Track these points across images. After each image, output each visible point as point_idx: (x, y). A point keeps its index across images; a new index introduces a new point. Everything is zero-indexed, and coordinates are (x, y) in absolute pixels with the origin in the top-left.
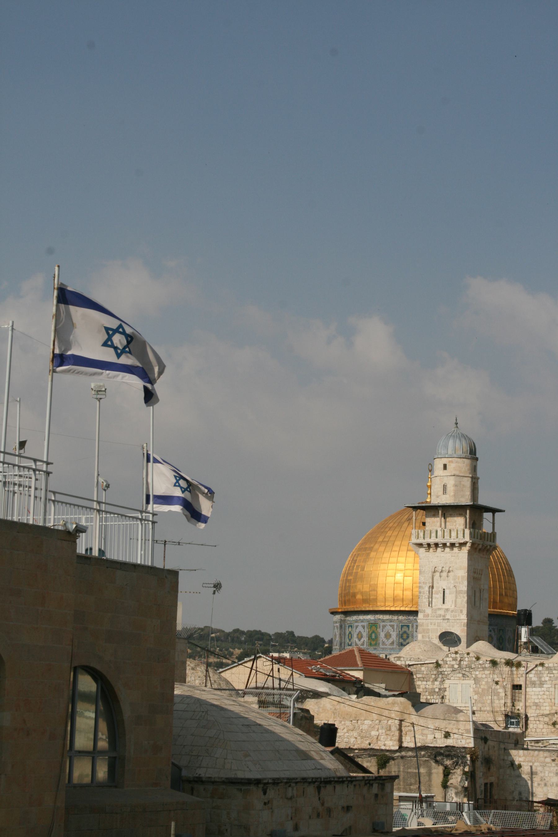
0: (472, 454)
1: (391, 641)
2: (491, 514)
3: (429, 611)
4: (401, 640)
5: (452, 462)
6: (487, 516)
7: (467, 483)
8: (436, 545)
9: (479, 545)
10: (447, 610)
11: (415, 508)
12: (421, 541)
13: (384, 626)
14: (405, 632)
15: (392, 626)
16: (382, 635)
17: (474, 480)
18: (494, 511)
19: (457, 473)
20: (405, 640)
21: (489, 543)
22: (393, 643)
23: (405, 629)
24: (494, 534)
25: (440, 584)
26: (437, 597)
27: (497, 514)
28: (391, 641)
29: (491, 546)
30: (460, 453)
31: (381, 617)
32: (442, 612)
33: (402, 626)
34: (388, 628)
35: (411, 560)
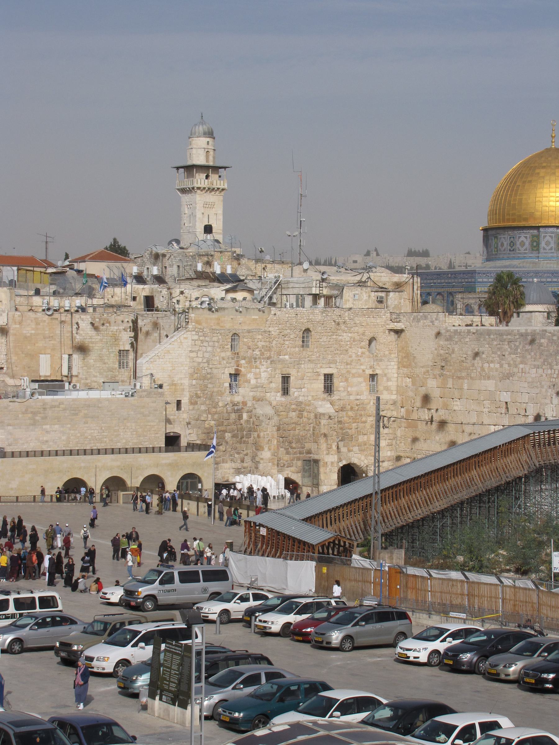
0: (210, 134)
1: (504, 248)
4: (509, 248)
5: (193, 140)
8: (184, 188)
9: (204, 188)
11: (178, 168)
14: (512, 242)
15: (504, 238)
16: (500, 244)
17: (207, 150)
18: (225, 168)
20: (512, 247)
22: (526, 249)
23: (512, 239)
28: (504, 248)
29: (218, 189)
31: (498, 231)
32: (188, 228)
33: (510, 238)
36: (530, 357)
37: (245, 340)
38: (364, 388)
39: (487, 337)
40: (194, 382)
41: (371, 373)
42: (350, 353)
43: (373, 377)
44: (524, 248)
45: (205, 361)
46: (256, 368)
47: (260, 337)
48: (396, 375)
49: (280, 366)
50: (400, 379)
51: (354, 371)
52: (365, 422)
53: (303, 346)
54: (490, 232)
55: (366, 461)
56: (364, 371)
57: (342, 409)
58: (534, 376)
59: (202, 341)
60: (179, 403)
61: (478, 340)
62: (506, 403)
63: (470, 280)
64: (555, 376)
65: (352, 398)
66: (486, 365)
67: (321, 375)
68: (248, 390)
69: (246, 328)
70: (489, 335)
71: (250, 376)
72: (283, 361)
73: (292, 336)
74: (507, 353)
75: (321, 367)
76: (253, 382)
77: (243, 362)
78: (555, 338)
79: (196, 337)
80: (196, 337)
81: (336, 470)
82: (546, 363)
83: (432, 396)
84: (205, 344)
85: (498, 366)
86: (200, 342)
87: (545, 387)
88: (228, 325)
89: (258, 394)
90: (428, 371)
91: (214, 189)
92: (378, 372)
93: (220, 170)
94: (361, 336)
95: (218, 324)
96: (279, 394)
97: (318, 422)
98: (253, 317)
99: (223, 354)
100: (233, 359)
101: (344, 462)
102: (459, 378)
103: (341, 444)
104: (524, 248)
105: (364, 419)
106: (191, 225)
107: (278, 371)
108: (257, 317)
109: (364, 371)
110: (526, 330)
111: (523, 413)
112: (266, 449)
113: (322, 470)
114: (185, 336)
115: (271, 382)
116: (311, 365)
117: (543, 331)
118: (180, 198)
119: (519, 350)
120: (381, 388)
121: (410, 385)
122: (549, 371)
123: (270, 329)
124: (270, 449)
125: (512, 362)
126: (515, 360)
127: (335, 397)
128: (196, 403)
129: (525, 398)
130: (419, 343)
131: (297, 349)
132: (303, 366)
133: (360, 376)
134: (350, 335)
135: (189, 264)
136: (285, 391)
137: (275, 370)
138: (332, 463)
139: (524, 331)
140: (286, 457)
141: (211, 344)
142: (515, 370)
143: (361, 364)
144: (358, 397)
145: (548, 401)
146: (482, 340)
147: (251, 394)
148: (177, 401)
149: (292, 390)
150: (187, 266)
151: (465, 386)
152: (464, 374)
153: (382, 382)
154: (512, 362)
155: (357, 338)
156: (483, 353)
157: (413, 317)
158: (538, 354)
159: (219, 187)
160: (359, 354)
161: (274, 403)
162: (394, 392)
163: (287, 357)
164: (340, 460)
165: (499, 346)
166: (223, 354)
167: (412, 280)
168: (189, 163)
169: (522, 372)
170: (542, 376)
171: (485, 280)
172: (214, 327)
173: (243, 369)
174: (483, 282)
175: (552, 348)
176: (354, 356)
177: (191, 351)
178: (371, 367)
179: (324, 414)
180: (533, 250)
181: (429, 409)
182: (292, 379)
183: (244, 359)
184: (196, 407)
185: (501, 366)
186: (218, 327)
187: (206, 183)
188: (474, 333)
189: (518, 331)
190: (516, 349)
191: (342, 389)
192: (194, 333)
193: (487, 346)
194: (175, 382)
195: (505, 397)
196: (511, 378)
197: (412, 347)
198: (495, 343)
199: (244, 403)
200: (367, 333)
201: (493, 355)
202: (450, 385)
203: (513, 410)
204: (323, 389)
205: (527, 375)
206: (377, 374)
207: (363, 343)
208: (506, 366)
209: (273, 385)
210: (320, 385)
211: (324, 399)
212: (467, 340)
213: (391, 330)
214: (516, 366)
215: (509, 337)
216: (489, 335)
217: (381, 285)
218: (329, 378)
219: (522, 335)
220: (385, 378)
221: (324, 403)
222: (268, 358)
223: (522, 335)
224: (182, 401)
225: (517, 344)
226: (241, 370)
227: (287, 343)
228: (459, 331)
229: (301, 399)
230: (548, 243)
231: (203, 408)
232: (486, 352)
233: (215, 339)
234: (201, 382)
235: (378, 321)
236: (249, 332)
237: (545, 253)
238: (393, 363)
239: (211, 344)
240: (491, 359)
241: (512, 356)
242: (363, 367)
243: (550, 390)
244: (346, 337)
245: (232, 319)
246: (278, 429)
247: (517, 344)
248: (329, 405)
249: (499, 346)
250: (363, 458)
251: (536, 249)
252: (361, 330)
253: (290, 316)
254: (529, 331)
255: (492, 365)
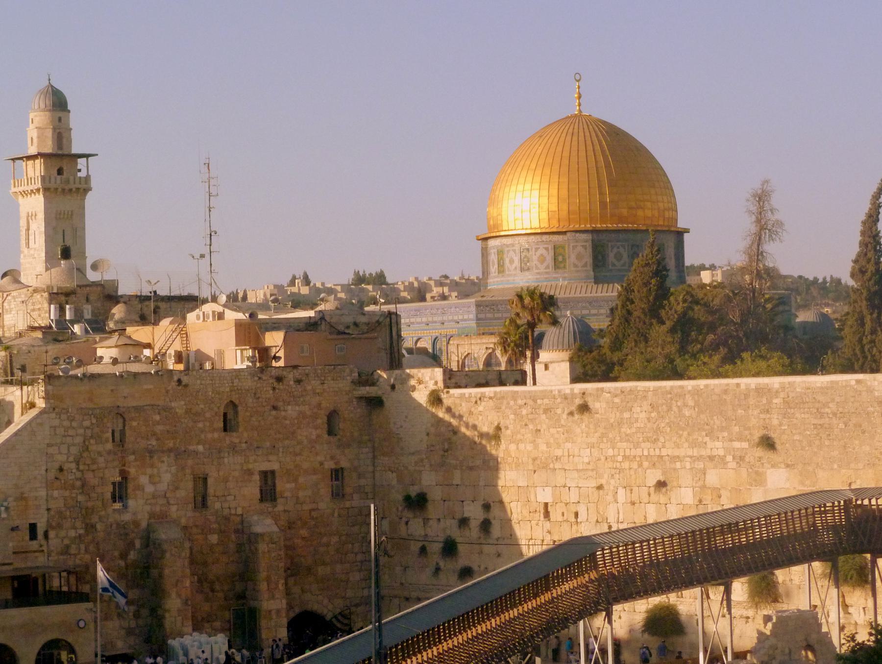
2: (85, 159)
3: (26, 250)
6: (81, 162)
7: (49, 133)
9: (57, 189)
10: (35, 249)
11: (13, 160)
12: (16, 190)
13: (508, 251)
16: (507, 261)
18: (87, 156)
19: (41, 125)
21: (78, 185)
22: (547, 267)
24: (87, 179)
25: (33, 226)
26: (31, 238)
27: (90, 158)
28: (514, 266)
29: (78, 189)
30: (42, 106)
32: (32, 252)
34: (512, 253)
35: (530, 178)
36: (578, 431)
37: (134, 424)
38: (323, 491)
39: (512, 403)
40: (56, 493)
41: (333, 467)
42: (299, 437)
43: (337, 474)
44: (545, 264)
45: (71, 459)
46: (152, 466)
47: (157, 418)
48: (370, 469)
49: (190, 462)
50: (377, 475)
51: (306, 465)
52: (328, 545)
53: (225, 430)
54: (491, 243)
55: (330, 607)
56: (321, 464)
57: (291, 525)
58: (586, 460)
59: (66, 429)
60: (33, 528)
61: (498, 408)
62: (546, 505)
63: (466, 317)
64: (620, 458)
65: (306, 507)
66: (513, 447)
67: (256, 473)
68: (141, 502)
69: (135, 404)
70: (515, 399)
71: (144, 480)
72: (196, 453)
73: (208, 415)
74: (544, 426)
75: (255, 461)
76: (150, 489)
77: (132, 457)
78: (617, 400)
79: (56, 422)
80: (56, 422)
81: (285, 621)
82: (605, 440)
83: (428, 497)
84: (71, 432)
85: (530, 447)
86: (62, 430)
87: (606, 476)
88: (107, 402)
89: (158, 509)
90: (422, 460)
91: (71, 190)
92: (344, 464)
93: (79, 160)
94: (315, 410)
95: (91, 400)
96: (191, 506)
97: (253, 548)
98: (145, 387)
99: (100, 448)
100: (115, 454)
101: (297, 610)
102: (471, 468)
103: (291, 581)
104: (545, 264)
105: (325, 540)
106: (37, 245)
107: (188, 471)
108: (151, 387)
109: (321, 464)
110: (572, 390)
111: (573, 520)
112: (174, 595)
113: (263, 623)
114: (39, 421)
115: (177, 488)
116: (239, 459)
117: (598, 389)
118: (18, 205)
119: (563, 422)
120: (348, 490)
121: (394, 482)
122: (610, 452)
123: (173, 404)
124: (179, 595)
125: (552, 441)
126: (557, 436)
127: (280, 508)
128: (59, 526)
129: (573, 497)
130: (406, 417)
131: (216, 435)
132: (226, 460)
133: (315, 472)
134: (297, 408)
135: (37, 307)
136: (202, 502)
137: (183, 469)
138: (278, 611)
139: (568, 391)
140: (206, 607)
141: (81, 431)
142: (559, 452)
143: (317, 454)
144: (313, 506)
145: (610, 498)
146: (503, 408)
147: (148, 508)
148: (31, 525)
149: (210, 500)
150: (33, 310)
151: (482, 483)
152: (478, 462)
153: (351, 482)
154: (552, 441)
155: (308, 413)
156: (507, 428)
157: (394, 376)
158: (591, 426)
159: (80, 186)
160: (314, 437)
161: (183, 521)
162: (370, 496)
163: (200, 448)
164: (290, 607)
165: (530, 417)
166: (100, 448)
167: (388, 319)
168: (33, 151)
169: (569, 456)
170: (599, 459)
171: (489, 315)
172: (84, 405)
173: (132, 471)
174: (486, 319)
175: (613, 416)
176: (305, 442)
177: (49, 445)
178: (332, 458)
179: (262, 535)
180: (558, 268)
181: (426, 521)
182: (210, 481)
183: (134, 453)
184: (62, 533)
185: (536, 447)
186: (91, 406)
187: (58, 182)
188: (491, 398)
189: (559, 391)
190: (559, 420)
191: (287, 494)
192: (53, 415)
193: (512, 416)
194: (26, 495)
195: (545, 495)
196: (551, 466)
197: (395, 423)
198: (524, 412)
199: (136, 524)
200: (324, 405)
201: (523, 431)
202: (457, 480)
203: (555, 515)
204: (259, 496)
205: (576, 459)
206: (342, 469)
207: (319, 421)
208: (543, 447)
209: (181, 493)
210: (253, 490)
211: (261, 513)
212: (481, 408)
213: (361, 398)
214: (559, 446)
215: (546, 401)
216: (515, 399)
217: (341, 328)
218: (268, 477)
219: (566, 398)
220: (354, 475)
221: (262, 517)
222: (170, 450)
223: (566, 398)
224: (39, 525)
225: (559, 411)
226: (129, 472)
227: (200, 425)
228: (467, 396)
229: (226, 512)
230: (579, 257)
231: (72, 533)
232: (511, 427)
233: (87, 423)
234: (67, 493)
235: (341, 385)
236: (137, 409)
237: (578, 271)
238: (365, 450)
239: (81, 431)
240: (519, 437)
241: (551, 430)
242: (320, 458)
243: (612, 482)
244: (291, 411)
245: (112, 391)
246: (192, 562)
247: (559, 411)
248: (269, 521)
249: (530, 417)
250: (326, 601)
251: (562, 265)
252: (315, 400)
253: (203, 382)
254: (576, 391)
255: (522, 446)
